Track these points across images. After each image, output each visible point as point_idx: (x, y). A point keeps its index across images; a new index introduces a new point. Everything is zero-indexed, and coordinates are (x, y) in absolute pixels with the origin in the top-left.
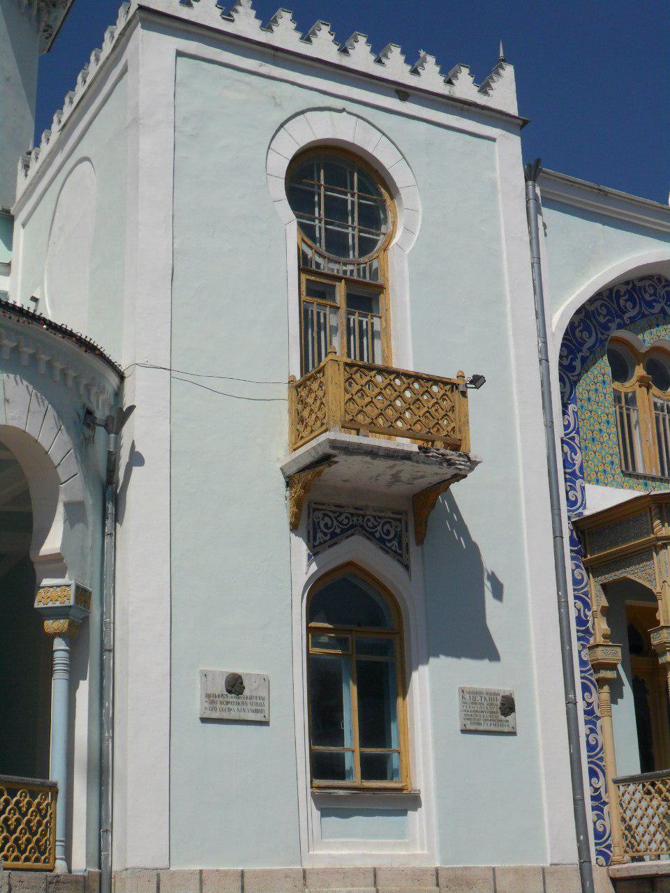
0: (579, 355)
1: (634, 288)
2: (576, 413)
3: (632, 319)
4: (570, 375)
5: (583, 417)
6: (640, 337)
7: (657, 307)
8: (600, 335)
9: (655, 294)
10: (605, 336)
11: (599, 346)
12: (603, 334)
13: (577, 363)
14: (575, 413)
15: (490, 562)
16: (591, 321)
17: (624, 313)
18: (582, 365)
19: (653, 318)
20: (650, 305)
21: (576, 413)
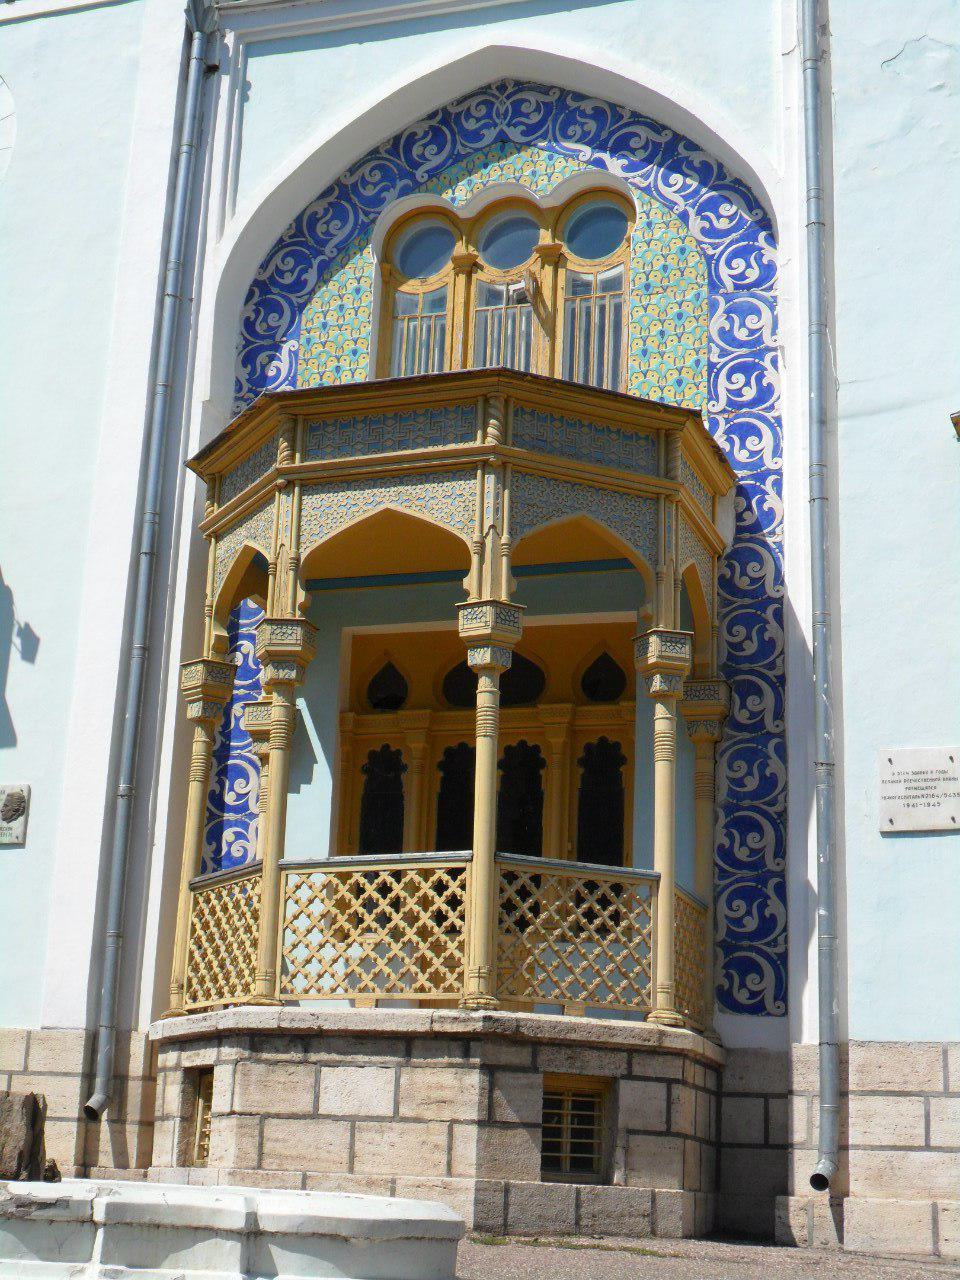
0: (316, 263)
1: (445, 121)
2: (296, 353)
3: (433, 173)
4: (291, 296)
5: (307, 356)
6: (447, 195)
7: (490, 135)
8: (362, 217)
9: (488, 115)
10: (372, 216)
11: (358, 235)
12: (366, 214)
13: (311, 276)
14: (294, 354)
15: (24, 611)
16: (349, 201)
17: (416, 165)
18: (320, 275)
19: (480, 155)
20: (476, 136)
21: (296, 353)
